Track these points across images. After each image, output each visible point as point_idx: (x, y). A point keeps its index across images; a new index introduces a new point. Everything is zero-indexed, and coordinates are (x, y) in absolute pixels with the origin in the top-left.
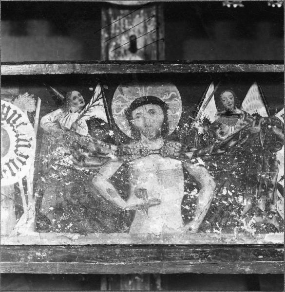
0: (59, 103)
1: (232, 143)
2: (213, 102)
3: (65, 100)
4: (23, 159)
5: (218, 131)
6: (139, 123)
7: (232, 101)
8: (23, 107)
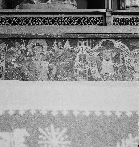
0: (14, 45)
1: (61, 57)
2: (56, 45)
3: (14, 44)
4: (2, 61)
5: (57, 54)
6: (35, 51)
7: (61, 45)
8: (3, 47)
